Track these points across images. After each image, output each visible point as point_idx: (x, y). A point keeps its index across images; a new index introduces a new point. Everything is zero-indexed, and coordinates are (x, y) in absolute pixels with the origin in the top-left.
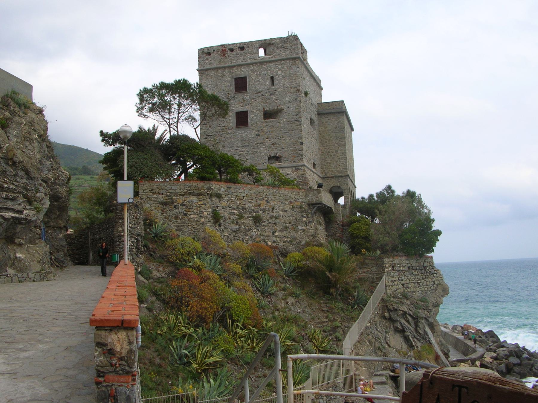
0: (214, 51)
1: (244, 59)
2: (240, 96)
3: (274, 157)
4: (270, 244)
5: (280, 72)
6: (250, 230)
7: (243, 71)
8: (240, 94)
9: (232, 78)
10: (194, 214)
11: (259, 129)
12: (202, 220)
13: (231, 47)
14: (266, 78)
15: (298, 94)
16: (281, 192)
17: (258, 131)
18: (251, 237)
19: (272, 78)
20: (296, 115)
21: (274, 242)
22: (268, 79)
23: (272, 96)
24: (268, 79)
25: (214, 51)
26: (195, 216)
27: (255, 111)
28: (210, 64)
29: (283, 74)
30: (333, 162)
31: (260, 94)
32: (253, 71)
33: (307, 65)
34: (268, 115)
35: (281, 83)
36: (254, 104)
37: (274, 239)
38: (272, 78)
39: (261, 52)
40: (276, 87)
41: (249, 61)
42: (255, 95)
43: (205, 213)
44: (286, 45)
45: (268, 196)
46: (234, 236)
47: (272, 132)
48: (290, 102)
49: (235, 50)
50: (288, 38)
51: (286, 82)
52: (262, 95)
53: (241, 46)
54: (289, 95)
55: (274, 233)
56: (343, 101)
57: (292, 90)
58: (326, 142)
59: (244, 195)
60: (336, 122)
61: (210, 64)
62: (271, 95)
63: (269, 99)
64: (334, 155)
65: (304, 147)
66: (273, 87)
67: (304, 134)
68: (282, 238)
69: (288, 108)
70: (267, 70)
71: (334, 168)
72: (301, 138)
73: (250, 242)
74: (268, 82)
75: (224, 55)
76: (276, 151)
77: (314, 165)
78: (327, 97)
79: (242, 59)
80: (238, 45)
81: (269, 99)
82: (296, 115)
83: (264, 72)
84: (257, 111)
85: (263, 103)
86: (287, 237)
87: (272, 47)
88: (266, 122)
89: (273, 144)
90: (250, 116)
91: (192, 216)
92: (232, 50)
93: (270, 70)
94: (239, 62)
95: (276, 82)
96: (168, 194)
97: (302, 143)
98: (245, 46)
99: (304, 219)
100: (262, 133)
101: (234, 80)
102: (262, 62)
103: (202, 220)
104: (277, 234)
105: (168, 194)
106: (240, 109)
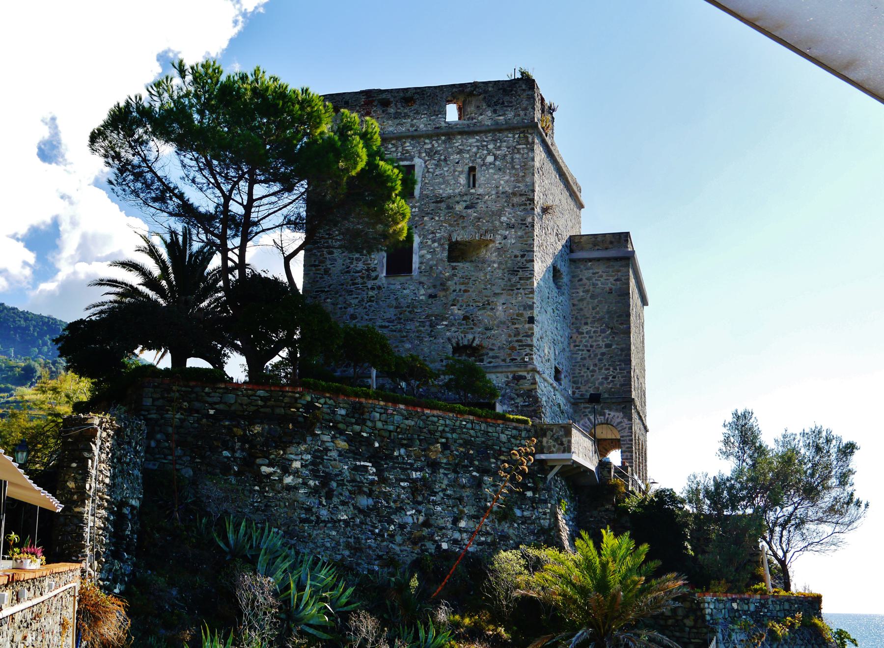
1: (412, 126)
3: (465, 347)
4: (445, 546)
6: (400, 509)
10: (268, 466)
12: (288, 480)
13: (384, 96)
14: (459, 169)
15: (529, 207)
16: (477, 427)
18: (402, 526)
19: (472, 169)
20: (523, 256)
21: (456, 542)
22: (461, 172)
23: (469, 211)
24: (461, 172)
26: (271, 470)
27: (430, 242)
30: (600, 369)
31: (443, 206)
33: (552, 148)
34: (458, 252)
35: (493, 182)
37: (457, 535)
38: (472, 169)
39: (452, 113)
40: (480, 191)
42: (432, 206)
43: (297, 465)
44: (507, 98)
45: (449, 435)
46: (362, 523)
48: (510, 226)
50: (513, 83)
51: (505, 181)
52: (449, 207)
53: (409, 94)
55: (455, 521)
56: (627, 234)
57: (516, 200)
58: (586, 324)
59: (391, 428)
60: (612, 279)
62: (467, 207)
63: (463, 217)
64: (603, 354)
65: (536, 329)
66: (473, 191)
67: (536, 298)
68: (473, 533)
69: (505, 238)
70: (460, 152)
71: (602, 384)
72: (531, 307)
73: (398, 539)
74: (462, 180)
76: (470, 337)
77: (557, 372)
78: (592, 223)
79: (409, 125)
80: (402, 95)
82: (523, 256)
84: (434, 242)
86: (487, 533)
88: (454, 268)
89: (466, 318)
91: (265, 469)
95: (481, 179)
96: (212, 412)
97: (531, 320)
98: (416, 96)
99: (529, 494)
100: (442, 294)
102: (450, 132)
103: (288, 480)
104: (462, 524)
105: (212, 412)
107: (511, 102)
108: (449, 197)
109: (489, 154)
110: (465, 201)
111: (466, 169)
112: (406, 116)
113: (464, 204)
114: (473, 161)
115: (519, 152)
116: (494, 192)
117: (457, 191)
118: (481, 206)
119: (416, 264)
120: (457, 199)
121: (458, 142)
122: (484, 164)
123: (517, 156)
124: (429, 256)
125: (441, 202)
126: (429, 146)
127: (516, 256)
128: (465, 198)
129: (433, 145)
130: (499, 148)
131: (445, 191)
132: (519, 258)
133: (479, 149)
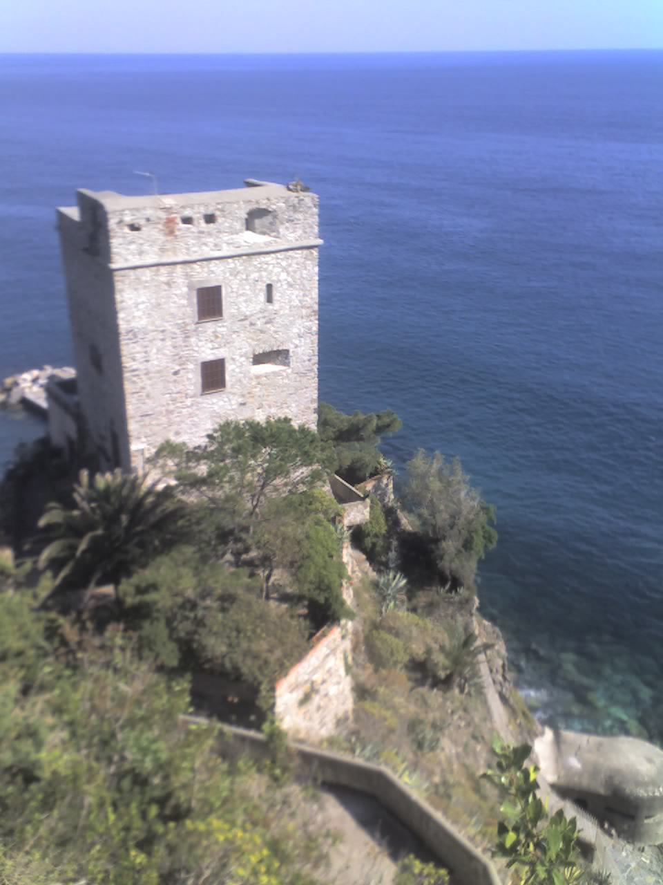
0: (148, 220)
1: (216, 245)
2: (210, 327)
5: (283, 276)
7: (213, 272)
8: (209, 325)
9: (190, 287)
11: (245, 392)
17: (243, 396)
19: (269, 287)
22: (261, 290)
23: (268, 326)
25: (148, 220)
28: (141, 253)
29: (290, 279)
31: (247, 323)
32: (234, 273)
36: (237, 344)
38: (269, 287)
41: (226, 251)
47: (268, 396)
49: (195, 222)
52: (252, 324)
54: (299, 321)
61: (141, 253)
62: (266, 323)
63: (262, 332)
66: (270, 307)
70: (260, 270)
75: (171, 232)
81: (262, 332)
82: (309, 360)
83: (255, 275)
85: (252, 339)
87: (269, 218)
90: (229, 367)
92: (187, 220)
93: (265, 270)
94: (208, 252)
95: (276, 296)
98: (217, 213)
100: (251, 400)
101: (194, 294)
106: (209, 355)
107: (299, 220)
108: (252, 315)
109: (283, 271)
110: (264, 317)
111: (265, 288)
112: (210, 234)
113: (264, 320)
114: (270, 279)
115: (306, 269)
116: (288, 307)
117: (258, 308)
118: (278, 320)
119: (227, 377)
120: (260, 315)
121: (256, 261)
122: (279, 281)
123: (305, 272)
124: (237, 370)
125: (245, 319)
126: (232, 265)
127: (304, 361)
128: (266, 314)
129: (235, 264)
130: (290, 265)
131: (246, 309)
132: (307, 362)
133: (274, 267)
